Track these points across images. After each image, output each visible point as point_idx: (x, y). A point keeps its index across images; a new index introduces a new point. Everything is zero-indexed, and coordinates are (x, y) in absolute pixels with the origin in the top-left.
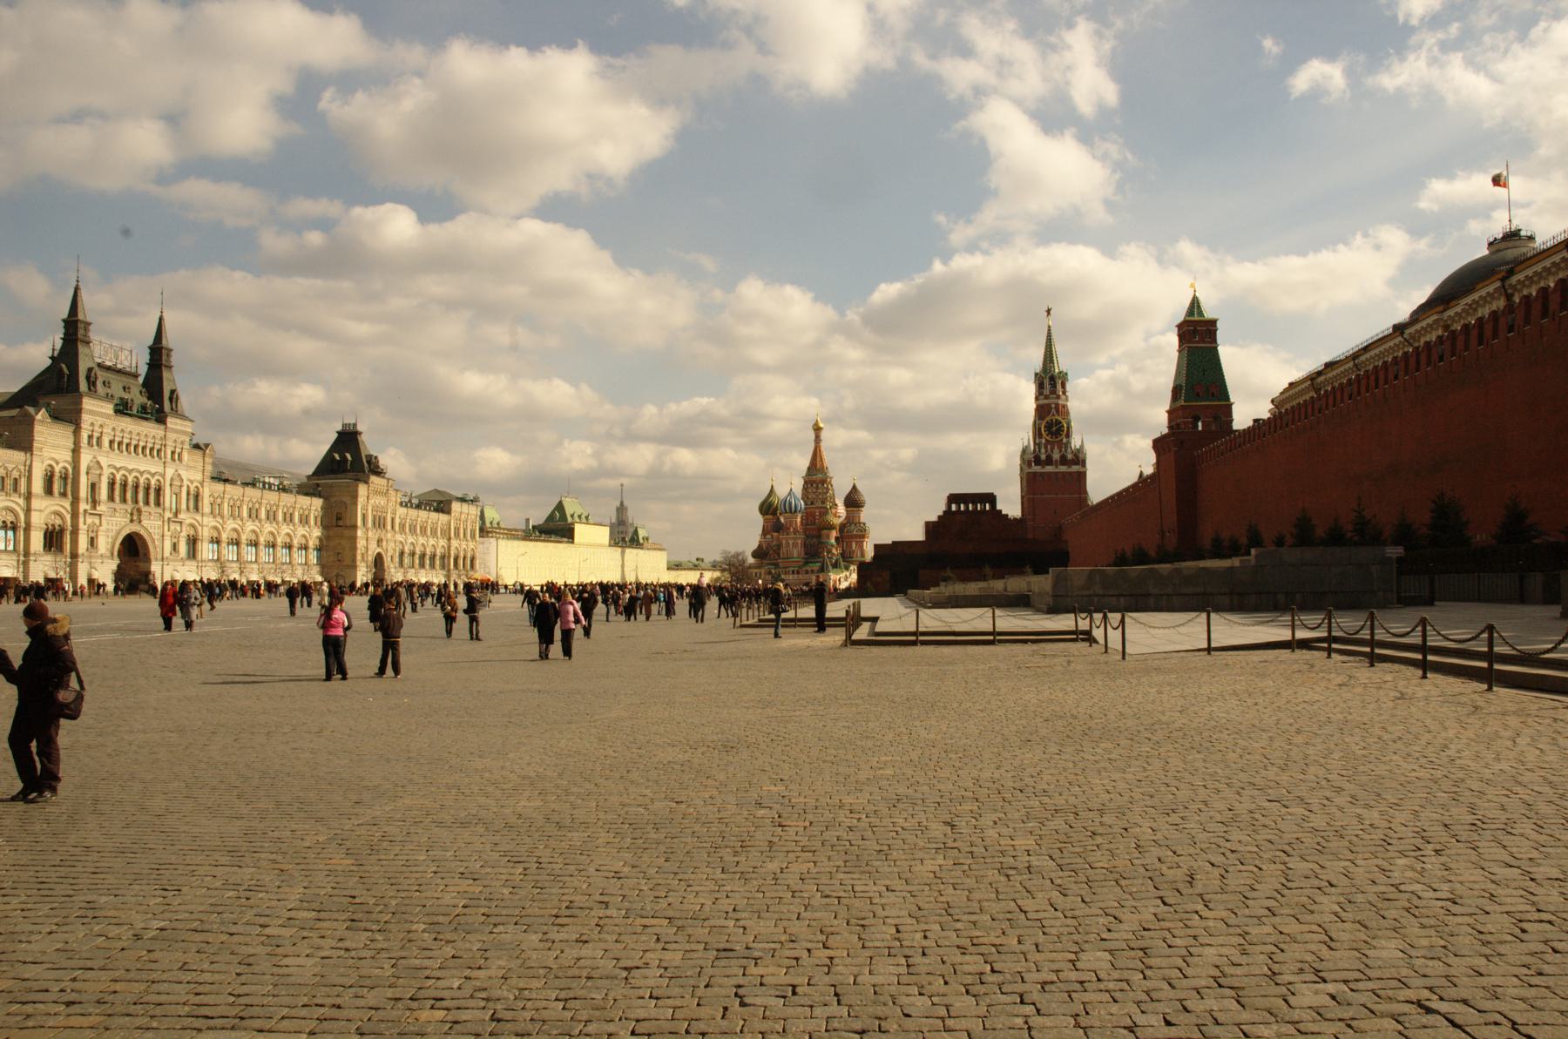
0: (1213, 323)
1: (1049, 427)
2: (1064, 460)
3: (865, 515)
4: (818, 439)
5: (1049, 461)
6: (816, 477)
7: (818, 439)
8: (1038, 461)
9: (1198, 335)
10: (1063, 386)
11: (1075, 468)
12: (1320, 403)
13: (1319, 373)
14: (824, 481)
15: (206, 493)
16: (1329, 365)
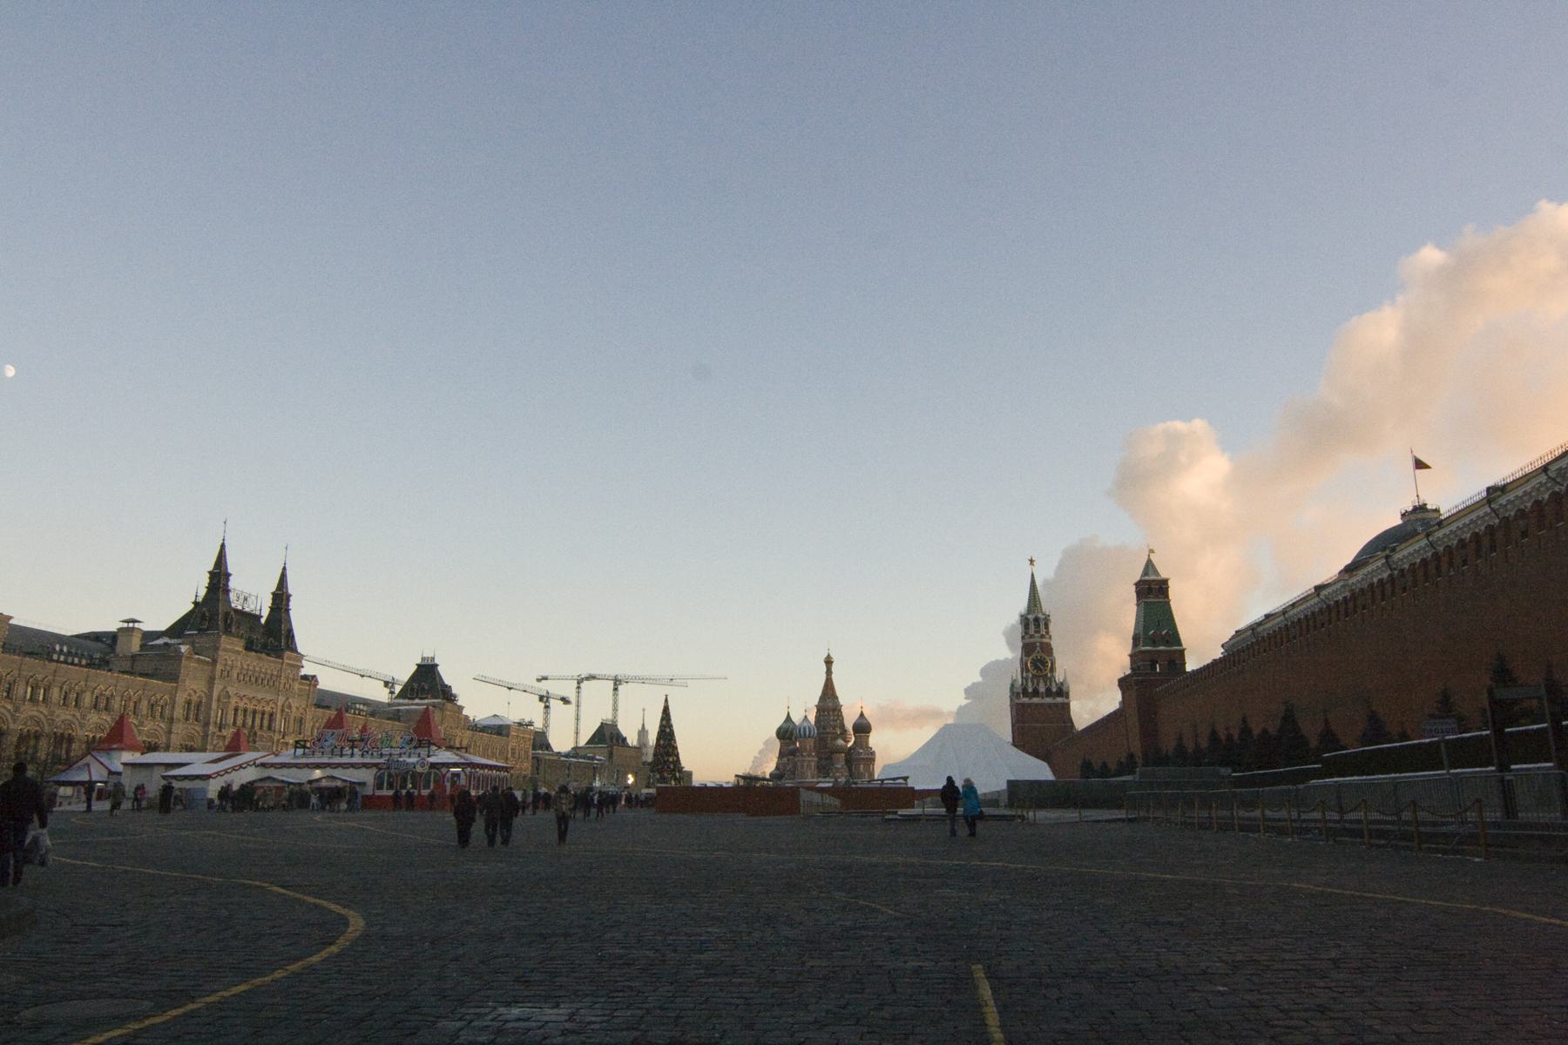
0: (1165, 582)
1: (1034, 663)
2: (1049, 693)
3: (874, 740)
4: (829, 672)
5: (1036, 693)
6: (828, 702)
7: (829, 672)
8: (1025, 692)
9: (1152, 592)
10: (1047, 626)
11: (1059, 700)
12: (1256, 648)
13: (1259, 624)
14: (837, 709)
15: (309, 716)
16: (1267, 616)
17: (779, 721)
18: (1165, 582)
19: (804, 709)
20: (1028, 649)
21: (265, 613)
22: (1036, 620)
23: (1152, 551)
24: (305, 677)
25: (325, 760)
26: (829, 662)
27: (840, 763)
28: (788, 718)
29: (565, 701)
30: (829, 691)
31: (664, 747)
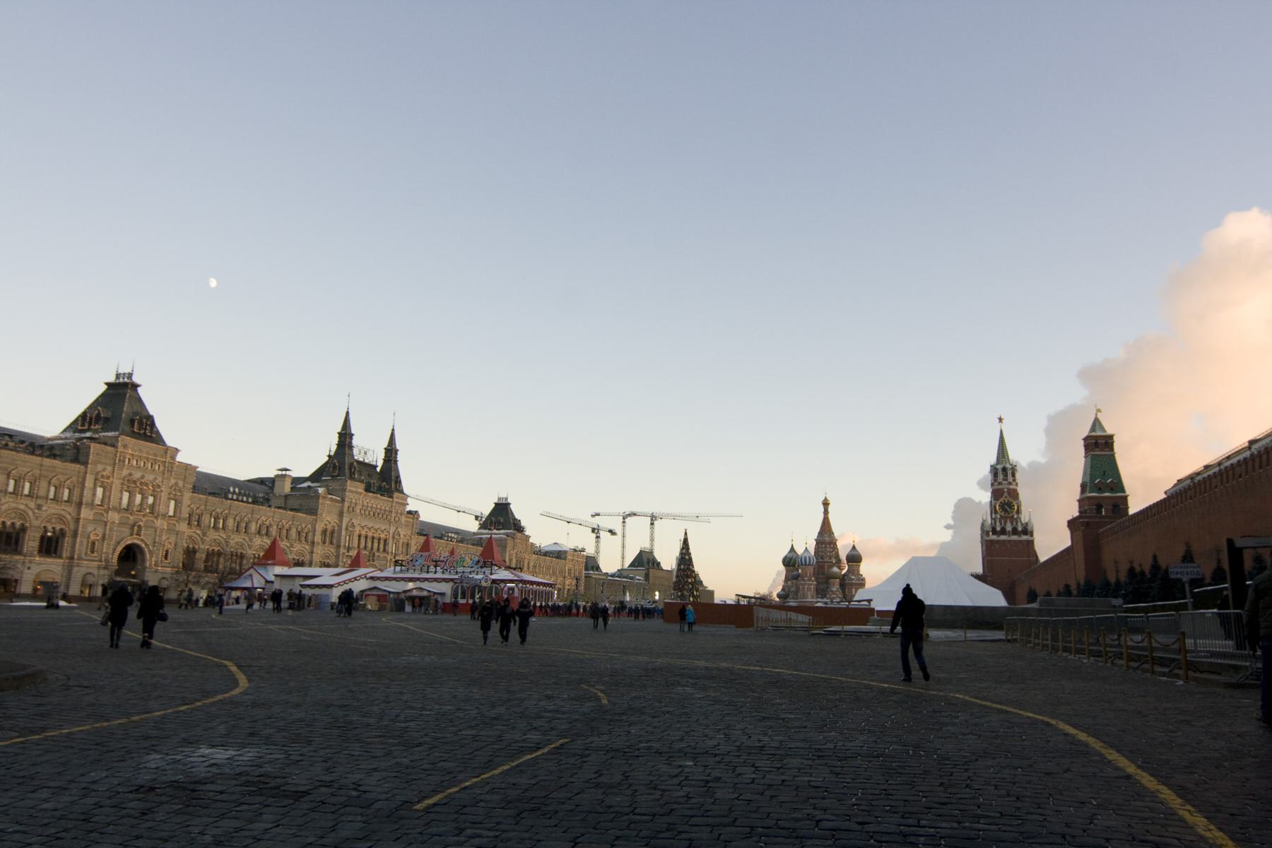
0: (1111, 437)
1: (1002, 506)
2: (1015, 531)
3: (865, 569)
4: (826, 512)
5: (1003, 531)
7: (826, 512)
9: (1099, 447)
10: (1013, 475)
11: (1024, 537)
12: (1196, 493)
13: (1198, 474)
14: (833, 543)
15: (413, 542)
16: (1206, 467)
17: (785, 552)
18: (1111, 437)
19: (806, 543)
20: (996, 494)
21: (380, 464)
22: (1004, 469)
23: (1099, 410)
24: (410, 512)
25: (416, 575)
26: (826, 504)
27: (835, 587)
28: (792, 549)
29: (612, 532)
30: (826, 527)
31: (684, 570)
